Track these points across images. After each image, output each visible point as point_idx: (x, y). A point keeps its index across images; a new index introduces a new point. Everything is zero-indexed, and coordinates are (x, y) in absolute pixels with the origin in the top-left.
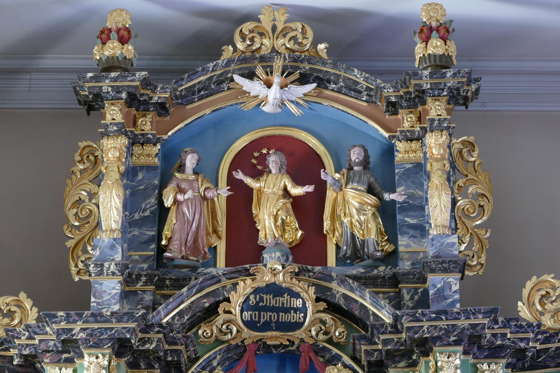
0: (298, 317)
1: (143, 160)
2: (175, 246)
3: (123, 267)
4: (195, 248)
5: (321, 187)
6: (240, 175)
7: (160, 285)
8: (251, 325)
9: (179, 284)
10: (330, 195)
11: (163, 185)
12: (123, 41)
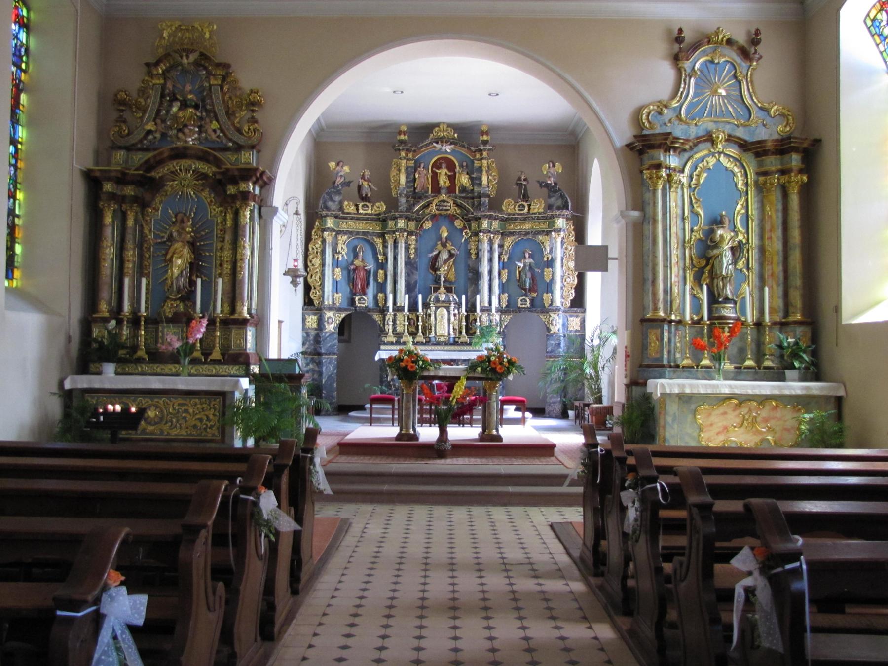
0: (449, 208)
1: (410, 165)
2: (418, 188)
3: (406, 195)
4: (423, 188)
5: (455, 174)
6: (434, 169)
7: (415, 198)
8: (437, 210)
9: (420, 198)
10: (457, 174)
11: (415, 172)
12: (405, 135)
